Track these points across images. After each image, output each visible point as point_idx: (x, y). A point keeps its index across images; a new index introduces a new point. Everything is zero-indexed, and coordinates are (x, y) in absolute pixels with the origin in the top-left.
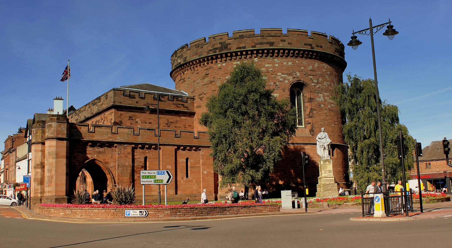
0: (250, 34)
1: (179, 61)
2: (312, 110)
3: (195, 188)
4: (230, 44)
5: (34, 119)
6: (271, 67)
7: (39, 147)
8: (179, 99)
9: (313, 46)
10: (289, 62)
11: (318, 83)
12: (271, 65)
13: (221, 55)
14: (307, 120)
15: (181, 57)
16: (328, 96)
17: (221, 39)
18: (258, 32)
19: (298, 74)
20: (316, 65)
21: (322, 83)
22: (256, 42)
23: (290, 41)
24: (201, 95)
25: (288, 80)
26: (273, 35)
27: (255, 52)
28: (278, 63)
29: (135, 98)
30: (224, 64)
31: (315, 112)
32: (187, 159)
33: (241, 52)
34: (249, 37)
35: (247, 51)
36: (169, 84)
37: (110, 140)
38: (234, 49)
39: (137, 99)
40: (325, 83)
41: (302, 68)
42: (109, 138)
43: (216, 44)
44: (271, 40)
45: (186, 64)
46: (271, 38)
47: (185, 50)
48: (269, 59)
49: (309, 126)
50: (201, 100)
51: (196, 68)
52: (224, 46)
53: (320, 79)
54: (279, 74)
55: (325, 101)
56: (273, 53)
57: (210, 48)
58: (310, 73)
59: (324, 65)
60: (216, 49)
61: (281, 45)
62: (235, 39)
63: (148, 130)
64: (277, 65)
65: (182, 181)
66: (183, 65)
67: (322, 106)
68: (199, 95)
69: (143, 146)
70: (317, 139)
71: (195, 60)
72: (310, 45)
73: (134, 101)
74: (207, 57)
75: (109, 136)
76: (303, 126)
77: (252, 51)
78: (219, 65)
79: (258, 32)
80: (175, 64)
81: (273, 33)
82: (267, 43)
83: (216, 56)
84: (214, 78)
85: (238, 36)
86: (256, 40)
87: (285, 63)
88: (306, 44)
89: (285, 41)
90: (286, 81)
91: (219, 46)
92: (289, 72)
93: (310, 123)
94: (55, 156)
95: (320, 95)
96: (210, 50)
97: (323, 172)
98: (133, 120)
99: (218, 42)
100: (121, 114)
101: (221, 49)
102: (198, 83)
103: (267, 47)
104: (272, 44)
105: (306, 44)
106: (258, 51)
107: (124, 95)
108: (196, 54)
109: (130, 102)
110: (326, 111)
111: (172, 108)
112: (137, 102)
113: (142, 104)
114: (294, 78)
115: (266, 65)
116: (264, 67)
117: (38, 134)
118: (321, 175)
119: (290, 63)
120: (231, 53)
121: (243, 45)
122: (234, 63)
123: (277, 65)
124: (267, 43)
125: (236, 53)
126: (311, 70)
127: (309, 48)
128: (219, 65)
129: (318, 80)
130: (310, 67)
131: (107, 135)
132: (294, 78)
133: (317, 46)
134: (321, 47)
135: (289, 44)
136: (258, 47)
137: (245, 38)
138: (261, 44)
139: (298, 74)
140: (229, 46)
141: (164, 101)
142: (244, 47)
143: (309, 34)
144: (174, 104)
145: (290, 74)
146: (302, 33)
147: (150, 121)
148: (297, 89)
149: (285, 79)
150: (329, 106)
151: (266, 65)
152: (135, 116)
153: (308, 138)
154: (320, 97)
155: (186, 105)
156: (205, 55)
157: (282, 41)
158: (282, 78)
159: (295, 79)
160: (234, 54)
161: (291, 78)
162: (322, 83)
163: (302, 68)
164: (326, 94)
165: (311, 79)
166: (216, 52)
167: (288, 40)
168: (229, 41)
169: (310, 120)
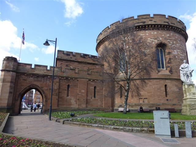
2: (170, 59)
3: (99, 104)
6: (144, 36)
8: (95, 57)
9: (169, 23)
10: (155, 33)
11: (173, 44)
12: (144, 35)
14: (167, 65)
16: (180, 52)
18: (136, 17)
19: (161, 39)
20: (172, 34)
21: (176, 44)
22: (135, 22)
23: (155, 20)
25: (155, 42)
26: (145, 18)
28: (148, 33)
29: (70, 56)
31: (172, 60)
32: (95, 87)
34: (131, 21)
36: (95, 53)
39: (71, 56)
40: (177, 45)
41: (163, 35)
42: (45, 73)
44: (144, 20)
46: (143, 19)
49: (169, 69)
53: (174, 42)
54: (148, 39)
55: (178, 54)
58: (168, 38)
59: (176, 35)
61: (150, 23)
63: (71, 69)
64: (147, 34)
65: (91, 100)
67: (177, 57)
69: (67, 78)
70: (180, 68)
72: (168, 23)
73: (69, 57)
75: (45, 71)
76: (165, 69)
79: (136, 17)
81: (145, 17)
82: (141, 22)
88: (164, 22)
89: (152, 20)
90: (153, 43)
92: (156, 38)
93: (169, 67)
94: (2, 81)
95: (175, 51)
97: (187, 94)
98: (68, 66)
99: (115, 26)
100: (62, 63)
103: (142, 24)
104: (144, 22)
105: (164, 22)
107: (64, 53)
110: (179, 60)
111: (91, 62)
112: (71, 58)
113: (73, 59)
114: (158, 41)
118: (186, 96)
119: (155, 33)
123: (147, 34)
124: (141, 22)
126: (168, 37)
127: (167, 24)
129: (173, 42)
130: (168, 35)
131: (44, 71)
132: (158, 41)
133: (172, 23)
134: (174, 24)
135: (154, 22)
137: (129, 22)
138: (138, 23)
139: (161, 39)
141: (87, 58)
143: (167, 17)
144: (92, 60)
145: (155, 39)
146: (162, 16)
147: (78, 68)
148: (160, 48)
149: (152, 41)
150: (181, 58)
151: (141, 35)
152: (70, 64)
153: (168, 75)
154: (175, 52)
155: (99, 61)
157: (150, 20)
158: (150, 41)
159: (159, 42)
161: (156, 41)
162: (176, 44)
163: (163, 35)
164: (179, 50)
165: (169, 41)
167: (154, 20)
169: (169, 65)
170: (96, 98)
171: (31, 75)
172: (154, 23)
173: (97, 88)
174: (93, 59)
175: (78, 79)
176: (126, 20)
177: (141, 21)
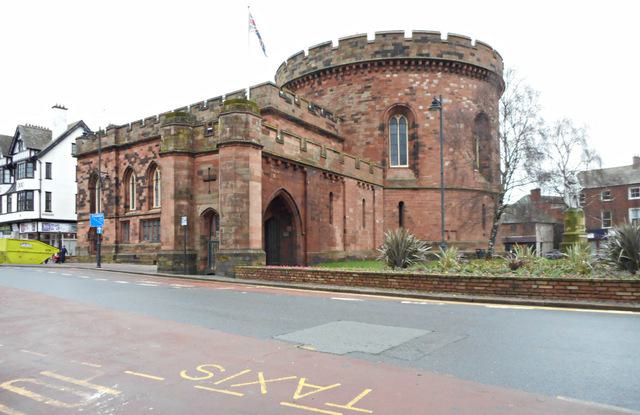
0: (434, 37)
1: (313, 65)
4: (408, 47)
5: (18, 134)
7: (185, 161)
12: (456, 85)
13: (395, 61)
15: (316, 59)
17: (395, 38)
24: (357, 115)
27: (441, 64)
30: (395, 75)
33: (424, 61)
35: (431, 61)
37: (299, 160)
38: (413, 55)
39: (293, 106)
43: (388, 45)
45: (330, 69)
47: (326, 49)
48: (454, 77)
50: (356, 121)
51: (346, 77)
52: (401, 48)
56: (461, 69)
57: (377, 49)
60: (389, 51)
62: (416, 41)
66: (324, 71)
68: (352, 115)
71: (350, 65)
74: (372, 63)
77: (438, 61)
78: (388, 76)
80: (303, 68)
81: (463, 42)
83: (387, 61)
84: (379, 93)
85: (419, 38)
86: (446, 48)
87: (470, 85)
89: (474, 55)
91: (392, 48)
96: (377, 53)
101: (394, 53)
102: (352, 98)
103: (455, 58)
104: (461, 56)
106: (445, 62)
108: (353, 55)
109: (286, 108)
111: (324, 127)
115: (452, 84)
116: (448, 86)
117: (181, 136)
120: (410, 60)
121: (425, 52)
122: (410, 75)
123: (462, 86)
125: (417, 60)
128: (388, 76)
135: (478, 60)
136: (445, 57)
138: (449, 53)
140: (406, 50)
142: (428, 55)
156: (367, 58)
158: (467, 104)
160: (413, 63)
166: (386, 56)
168: (407, 44)
170: (366, 230)
171: (279, 162)
172: (477, 64)
173: (367, 204)
174: (327, 120)
175: (345, 179)
176: (424, 36)
177: (453, 50)
